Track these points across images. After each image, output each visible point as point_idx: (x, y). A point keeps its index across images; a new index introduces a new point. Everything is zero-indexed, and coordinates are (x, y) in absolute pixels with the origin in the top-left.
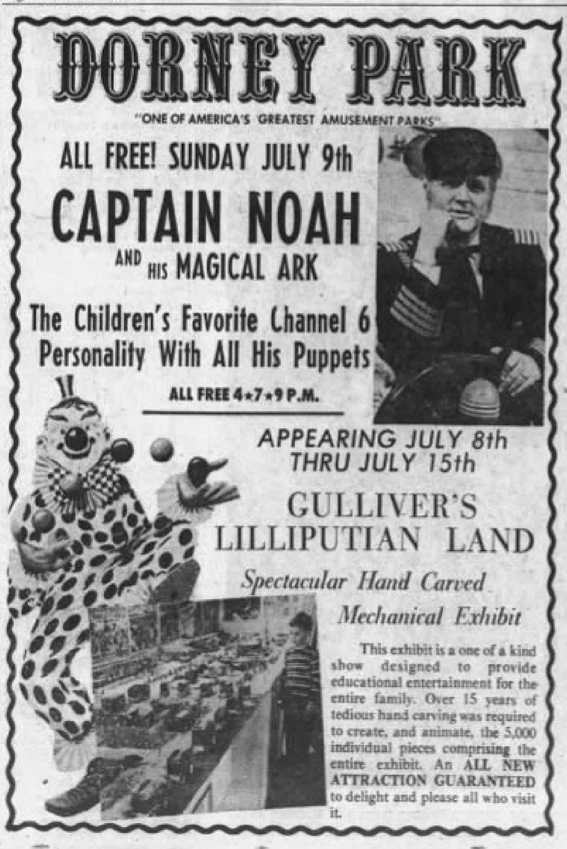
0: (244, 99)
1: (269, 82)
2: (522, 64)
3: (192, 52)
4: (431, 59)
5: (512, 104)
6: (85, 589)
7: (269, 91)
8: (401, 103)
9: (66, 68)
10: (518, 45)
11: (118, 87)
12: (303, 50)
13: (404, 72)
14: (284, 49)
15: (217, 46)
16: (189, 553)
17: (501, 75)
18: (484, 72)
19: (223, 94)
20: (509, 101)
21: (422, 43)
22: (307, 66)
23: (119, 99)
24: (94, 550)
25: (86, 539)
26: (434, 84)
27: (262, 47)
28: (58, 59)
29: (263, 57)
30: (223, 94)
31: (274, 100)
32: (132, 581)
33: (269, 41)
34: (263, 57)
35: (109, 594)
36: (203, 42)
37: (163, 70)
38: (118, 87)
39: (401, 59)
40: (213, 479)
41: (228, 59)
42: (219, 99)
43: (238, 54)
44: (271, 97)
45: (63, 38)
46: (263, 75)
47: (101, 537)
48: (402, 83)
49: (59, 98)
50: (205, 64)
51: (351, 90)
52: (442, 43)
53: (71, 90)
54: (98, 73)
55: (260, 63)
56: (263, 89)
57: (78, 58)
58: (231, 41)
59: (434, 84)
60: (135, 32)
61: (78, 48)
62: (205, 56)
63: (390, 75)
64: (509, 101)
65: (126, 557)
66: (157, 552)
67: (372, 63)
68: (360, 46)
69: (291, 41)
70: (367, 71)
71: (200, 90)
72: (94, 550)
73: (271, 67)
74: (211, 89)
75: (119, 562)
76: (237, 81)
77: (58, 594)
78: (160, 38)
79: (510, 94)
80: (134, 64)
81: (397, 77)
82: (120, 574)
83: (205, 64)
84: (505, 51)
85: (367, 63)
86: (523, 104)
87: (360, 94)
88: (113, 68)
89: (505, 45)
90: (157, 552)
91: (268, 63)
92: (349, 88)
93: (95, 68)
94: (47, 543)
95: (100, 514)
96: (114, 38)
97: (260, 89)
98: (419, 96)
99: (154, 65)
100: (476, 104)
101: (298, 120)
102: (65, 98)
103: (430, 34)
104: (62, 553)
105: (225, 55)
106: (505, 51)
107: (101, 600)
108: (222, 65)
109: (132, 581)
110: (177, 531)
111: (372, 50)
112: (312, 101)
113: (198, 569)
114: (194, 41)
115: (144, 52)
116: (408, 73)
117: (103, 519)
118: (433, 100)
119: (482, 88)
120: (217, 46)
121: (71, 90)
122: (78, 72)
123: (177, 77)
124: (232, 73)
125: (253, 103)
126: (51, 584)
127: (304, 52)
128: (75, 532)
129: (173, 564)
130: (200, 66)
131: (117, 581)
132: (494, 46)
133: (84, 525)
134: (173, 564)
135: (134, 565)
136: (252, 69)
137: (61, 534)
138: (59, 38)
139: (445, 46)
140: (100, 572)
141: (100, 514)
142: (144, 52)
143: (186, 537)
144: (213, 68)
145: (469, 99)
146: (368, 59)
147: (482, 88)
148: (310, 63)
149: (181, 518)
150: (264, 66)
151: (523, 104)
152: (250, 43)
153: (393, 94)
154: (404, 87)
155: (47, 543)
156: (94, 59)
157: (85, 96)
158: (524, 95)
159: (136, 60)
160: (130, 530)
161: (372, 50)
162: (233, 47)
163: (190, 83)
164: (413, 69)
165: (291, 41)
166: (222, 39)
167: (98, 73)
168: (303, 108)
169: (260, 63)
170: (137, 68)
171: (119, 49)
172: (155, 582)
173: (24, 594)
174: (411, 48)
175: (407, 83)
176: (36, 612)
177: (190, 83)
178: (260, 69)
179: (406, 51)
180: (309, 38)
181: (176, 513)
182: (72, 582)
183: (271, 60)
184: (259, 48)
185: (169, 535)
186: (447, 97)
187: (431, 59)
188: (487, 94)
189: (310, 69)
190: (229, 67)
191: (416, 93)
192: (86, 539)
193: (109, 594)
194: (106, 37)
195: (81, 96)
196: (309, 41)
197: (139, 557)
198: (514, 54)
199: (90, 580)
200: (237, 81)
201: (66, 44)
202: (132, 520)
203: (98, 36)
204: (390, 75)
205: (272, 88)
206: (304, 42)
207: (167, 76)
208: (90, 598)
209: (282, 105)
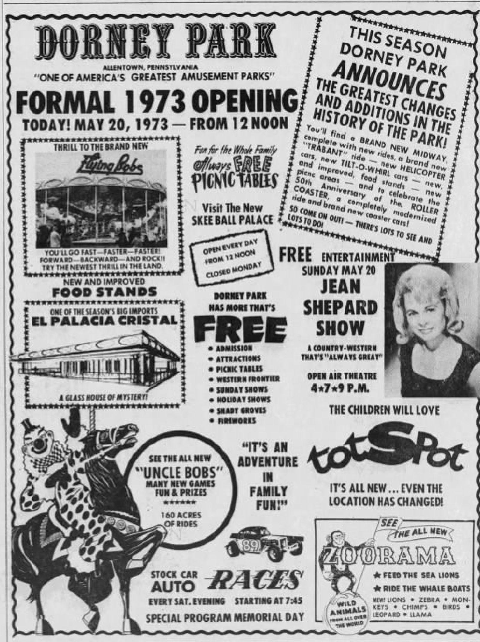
0: (133, 57)
3: (105, 34)
4: (228, 35)
8: (213, 57)
9: (42, 43)
10: (272, 27)
11: (69, 52)
14: (153, 33)
15: (118, 31)
19: (122, 55)
21: (223, 27)
26: (229, 47)
28: (37, 39)
29: (142, 35)
34: (142, 35)
37: (91, 43)
42: (120, 58)
43: (129, 35)
46: (143, 45)
49: (39, 58)
51: (187, 51)
52: (233, 26)
53: (44, 55)
54: (58, 46)
56: (142, 52)
58: (126, 28)
59: (229, 47)
67: (198, 37)
68: (191, 28)
69: (156, 27)
71: (110, 53)
76: (129, 48)
79: (269, 51)
81: (211, 44)
84: (265, 30)
86: (275, 56)
87: (192, 53)
89: (265, 27)
92: (187, 50)
96: (66, 28)
97: (141, 52)
98: (222, 54)
99: (86, 41)
100: (251, 57)
101: (163, 77)
102: (41, 59)
103: (227, 22)
105: (123, 34)
106: (265, 30)
108: (121, 40)
111: (198, 31)
112: (168, 57)
115: (81, 35)
119: (254, 48)
121: (44, 55)
122: (48, 45)
123: (98, 47)
125: (137, 59)
127: (163, 32)
130: (110, 41)
136: (137, 41)
139: (236, 28)
142: (81, 35)
145: (248, 54)
146: (196, 35)
147: (254, 48)
152: (136, 29)
153: (209, 53)
158: (276, 51)
161: (198, 31)
162: (126, 31)
163: (105, 50)
164: (219, 40)
167: (58, 46)
168: (163, 61)
171: (69, 32)
174: (218, 29)
177: (105, 50)
184: (140, 31)
186: (236, 53)
187: (228, 35)
188: (257, 51)
190: (125, 41)
191: (220, 52)
194: (61, 28)
195: (49, 58)
198: (269, 32)
200: (129, 48)
201: (42, 31)
204: (206, 44)
205: (148, 51)
206: (163, 28)
209: (153, 60)
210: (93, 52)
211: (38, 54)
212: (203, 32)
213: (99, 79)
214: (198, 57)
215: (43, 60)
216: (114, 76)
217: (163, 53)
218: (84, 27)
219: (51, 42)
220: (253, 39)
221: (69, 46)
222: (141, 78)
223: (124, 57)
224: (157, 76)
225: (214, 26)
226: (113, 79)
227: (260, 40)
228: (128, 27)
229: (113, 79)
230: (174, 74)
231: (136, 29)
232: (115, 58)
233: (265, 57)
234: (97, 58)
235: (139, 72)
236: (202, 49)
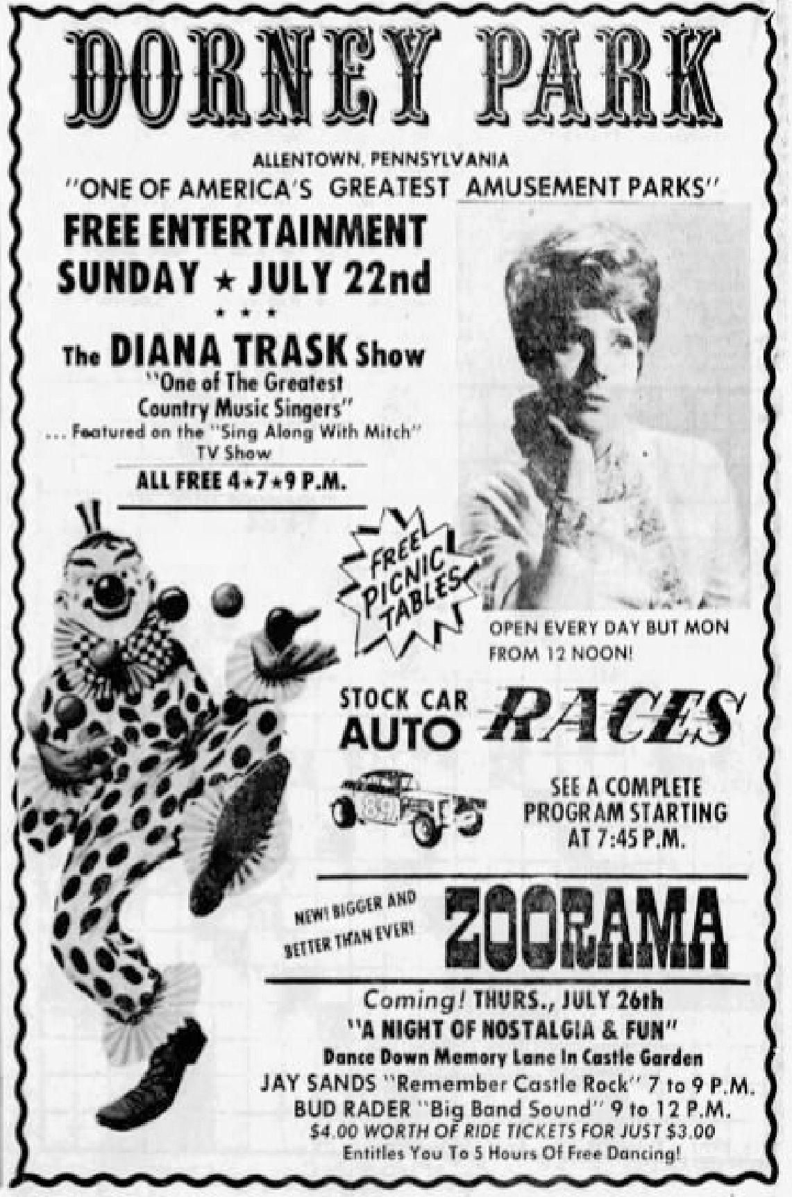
1: (364, 96)
2: (716, 66)
4: (590, 60)
5: (703, 123)
6: (132, 805)
7: (364, 109)
8: (550, 123)
9: (83, 79)
11: (155, 105)
12: (410, 47)
13: (552, 77)
14: (385, 50)
15: (292, 45)
16: (275, 743)
17: (687, 80)
18: (664, 76)
19: (301, 116)
20: (698, 119)
22: (415, 71)
23: (157, 123)
24: (142, 749)
25: (131, 734)
26: (594, 97)
27: (353, 45)
28: (72, 68)
29: (355, 59)
30: (301, 116)
31: (372, 121)
32: (197, 790)
33: (363, 36)
34: (355, 59)
35: (166, 810)
36: (274, 41)
37: (216, 80)
38: (155, 105)
39: (548, 59)
40: (303, 637)
41: (307, 64)
42: (297, 121)
43: (321, 56)
44: (367, 116)
45: (77, 36)
46: (356, 86)
47: (151, 730)
48: (550, 94)
49: (74, 124)
50: (275, 71)
51: (481, 106)
53: (88, 113)
54: (127, 86)
55: (351, 69)
56: (356, 105)
57: (99, 64)
58: (311, 38)
59: (594, 97)
60: (177, 27)
61: (99, 50)
62: (274, 60)
63: (533, 81)
64: (698, 119)
65: (187, 757)
66: (229, 747)
70: (502, 77)
71: (269, 110)
72: (142, 749)
73: (364, 73)
74: (286, 107)
75: (176, 766)
76: (321, 94)
77: (97, 814)
78: (211, 33)
79: (701, 108)
80: (176, 72)
81: (544, 84)
82: (181, 781)
83: (275, 71)
84: (693, 46)
85: (501, 66)
86: (719, 123)
88: (148, 78)
89: (691, 38)
90: (229, 747)
91: (361, 68)
93: (124, 78)
94: (76, 743)
95: (149, 696)
96: (151, 35)
97: (353, 106)
99: (203, 73)
103: (589, 25)
104: (98, 756)
105: (304, 56)
106: (693, 46)
107: (156, 820)
108: (299, 71)
109: (197, 790)
110: (254, 714)
113: (288, 766)
114: (260, 38)
115: (189, 57)
116: (559, 80)
117: (152, 705)
118: (593, 117)
119: (661, 102)
120: (292, 45)
121: (88, 113)
122: (100, 86)
124: (313, 82)
126: (86, 802)
127: (411, 52)
128: (115, 725)
129: (252, 762)
130: (269, 72)
131: (176, 790)
132: (677, 40)
133: (128, 715)
134: (252, 762)
135: (197, 769)
137: (97, 728)
138: (72, 37)
140: (153, 779)
141: (149, 696)
142: (189, 57)
143: (268, 723)
144: (286, 75)
147: (661, 102)
148: (419, 67)
149: (260, 697)
150: (356, 72)
151: (719, 123)
152: (339, 40)
153: (538, 110)
154: (553, 99)
155: (76, 743)
156: (121, 68)
157: (110, 120)
158: (720, 109)
159: (178, 67)
160: (190, 718)
162: (313, 46)
163: (255, 101)
164: (565, 75)
165: (390, 34)
166: (299, 35)
169: (351, 69)
170: (180, 77)
171: (156, 49)
172: (229, 789)
173: (51, 816)
174: (564, 42)
175: (559, 94)
176: (68, 840)
178: (350, 78)
179: (555, 49)
180: (419, 31)
181: (252, 688)
182: (115, 797)
183: (364, 63)
185: (245, 719)
186: (613, 111)
187: (590, 60)
188: (668, 108)
189: (419, 77)
190: (309, 74)
192: (131, 734)
193: (166, 810)
195: (104, 122)
196: (418, 35)
197: (204, 754)
199: (139, 792)
200: (321, 94)
201: (83, 44)
202: (193, 703)
203: (126, 32)
204: (533, 81)
207: (222, 88)
208: (141, 817)
210: (223, 107)
211: (72, 110)
212: (522, 53)
213: (239, 191)
214: (505, 123)
215: (86, 128)
216: (283, 183)
217: (412, 109)
218: (194, 35)
219: (109, 76)
220: (658, 72)
221: (156, 87)
222: (355, 189)
223: (307, 121)
224: (396, 186)
225: (552, 36)
226: (279, 193)
227: (676, 74)
228: (319, 35)
229: (279, 193)
230: (444, 180)
231: (339, 40)
232: (283, 122)
233: (692, 123)
234: (232, 123)
235: (348, 171)
236: (519, 101)
